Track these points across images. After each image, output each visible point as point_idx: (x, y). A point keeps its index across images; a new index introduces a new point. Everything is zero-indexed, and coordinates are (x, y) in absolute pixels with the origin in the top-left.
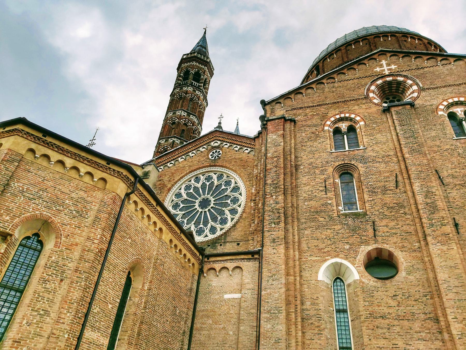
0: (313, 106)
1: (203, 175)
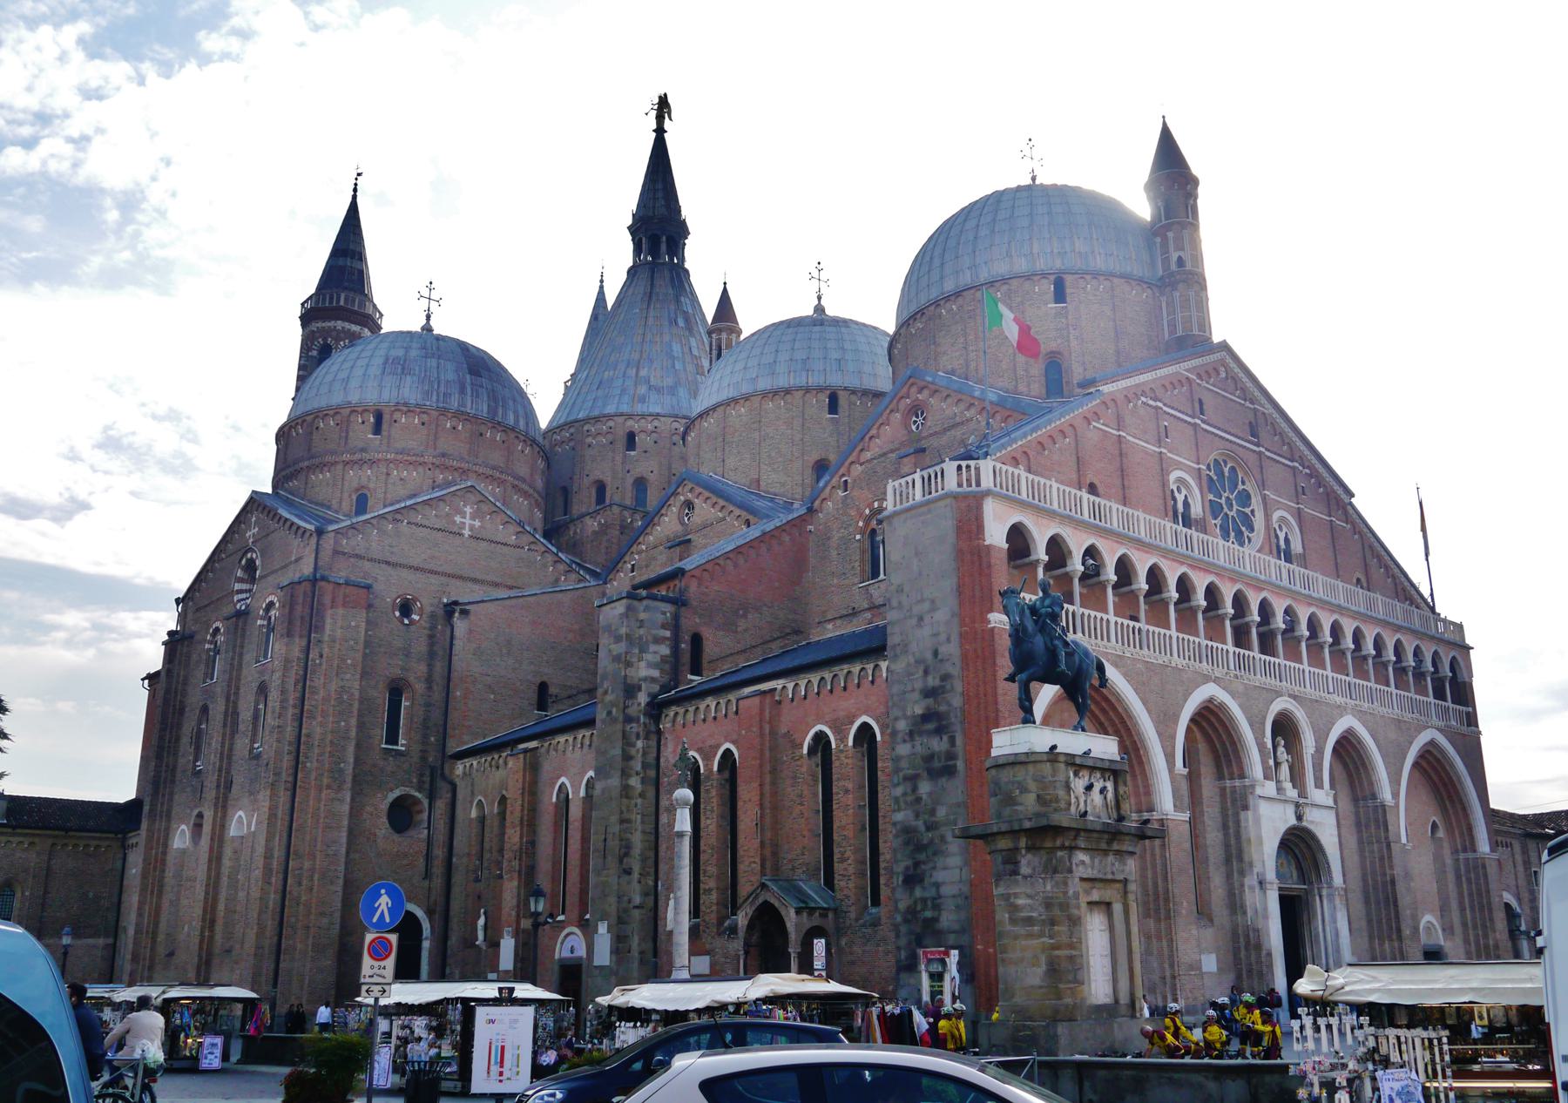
0: (206, 606)
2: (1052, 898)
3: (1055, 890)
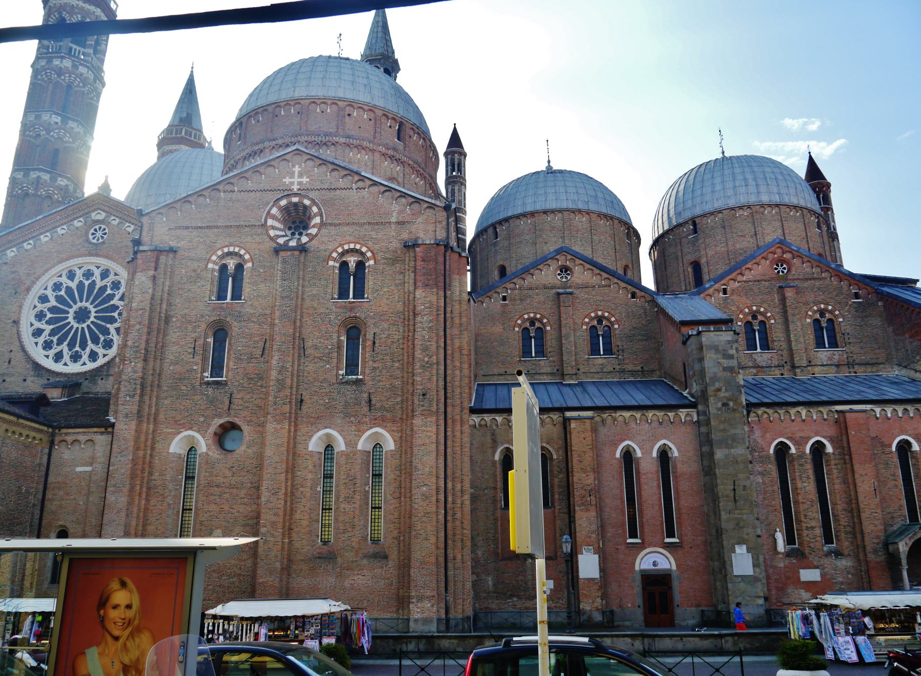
0: (201, 228)
1: (80, 268)
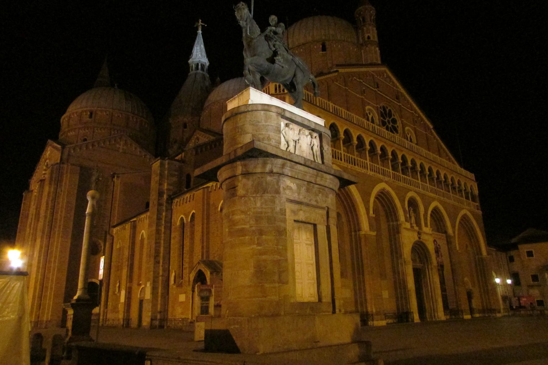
2: (261, 213)
3: (264, 206)
